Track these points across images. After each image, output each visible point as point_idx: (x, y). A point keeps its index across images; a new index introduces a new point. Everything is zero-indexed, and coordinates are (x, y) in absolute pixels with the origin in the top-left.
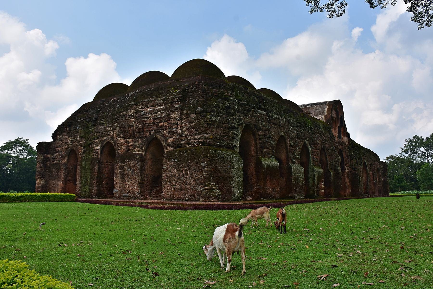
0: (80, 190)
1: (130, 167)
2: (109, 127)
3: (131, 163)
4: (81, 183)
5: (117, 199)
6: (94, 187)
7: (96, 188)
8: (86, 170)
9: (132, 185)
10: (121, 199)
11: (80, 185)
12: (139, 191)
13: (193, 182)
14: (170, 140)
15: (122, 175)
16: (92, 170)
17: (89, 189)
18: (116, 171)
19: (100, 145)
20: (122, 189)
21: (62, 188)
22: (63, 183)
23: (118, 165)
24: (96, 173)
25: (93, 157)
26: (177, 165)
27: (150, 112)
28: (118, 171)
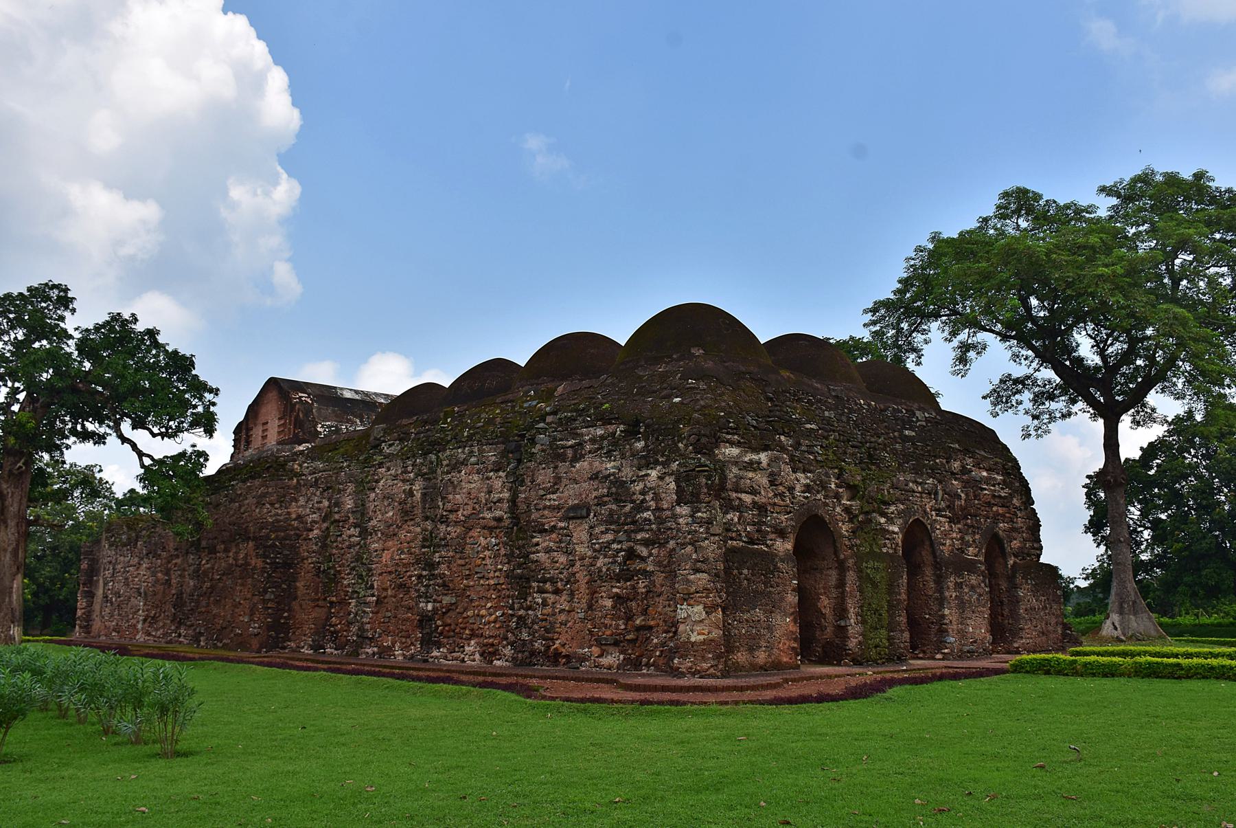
0: (860, 643)
1: (972, 588)
2: (915, 482)
3: (974, 579)
4: (864, 622)
5: (955, 659)
6: (902, 631)
7: (907, 635)
8: (875, 585)
9: (978, 628)
10: (960, 658)
11: (859, 628)
12: (989, 637)
13: (1053, 621)
14: (1016, 544)
15: (962, 605)
16: (892, 588)
17: (889, 639)
18: (947, 594)
19: (900, 521)
20: (962, 634)
21: (795, 640)
22: (795, 621)
23: (951, 581)
24: (904, 596)
25: (884, 550)
26: (1035, 591)
27: (987, 481)
28: (951, 594)
